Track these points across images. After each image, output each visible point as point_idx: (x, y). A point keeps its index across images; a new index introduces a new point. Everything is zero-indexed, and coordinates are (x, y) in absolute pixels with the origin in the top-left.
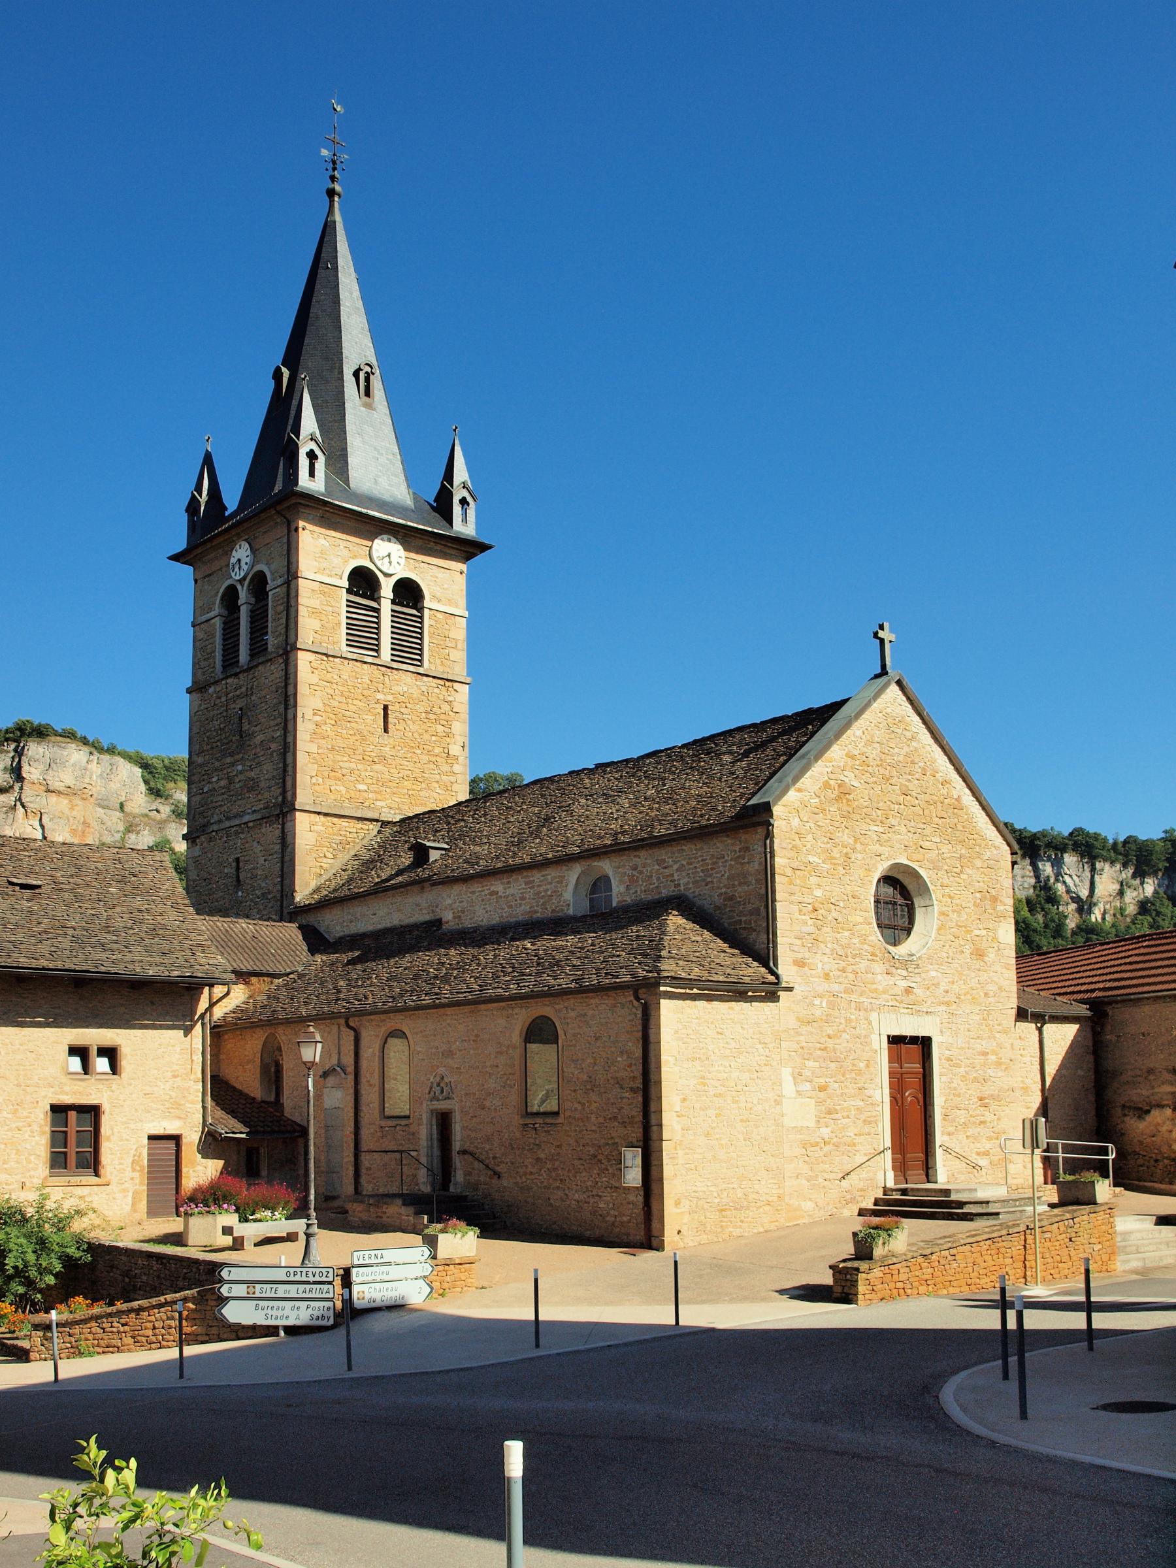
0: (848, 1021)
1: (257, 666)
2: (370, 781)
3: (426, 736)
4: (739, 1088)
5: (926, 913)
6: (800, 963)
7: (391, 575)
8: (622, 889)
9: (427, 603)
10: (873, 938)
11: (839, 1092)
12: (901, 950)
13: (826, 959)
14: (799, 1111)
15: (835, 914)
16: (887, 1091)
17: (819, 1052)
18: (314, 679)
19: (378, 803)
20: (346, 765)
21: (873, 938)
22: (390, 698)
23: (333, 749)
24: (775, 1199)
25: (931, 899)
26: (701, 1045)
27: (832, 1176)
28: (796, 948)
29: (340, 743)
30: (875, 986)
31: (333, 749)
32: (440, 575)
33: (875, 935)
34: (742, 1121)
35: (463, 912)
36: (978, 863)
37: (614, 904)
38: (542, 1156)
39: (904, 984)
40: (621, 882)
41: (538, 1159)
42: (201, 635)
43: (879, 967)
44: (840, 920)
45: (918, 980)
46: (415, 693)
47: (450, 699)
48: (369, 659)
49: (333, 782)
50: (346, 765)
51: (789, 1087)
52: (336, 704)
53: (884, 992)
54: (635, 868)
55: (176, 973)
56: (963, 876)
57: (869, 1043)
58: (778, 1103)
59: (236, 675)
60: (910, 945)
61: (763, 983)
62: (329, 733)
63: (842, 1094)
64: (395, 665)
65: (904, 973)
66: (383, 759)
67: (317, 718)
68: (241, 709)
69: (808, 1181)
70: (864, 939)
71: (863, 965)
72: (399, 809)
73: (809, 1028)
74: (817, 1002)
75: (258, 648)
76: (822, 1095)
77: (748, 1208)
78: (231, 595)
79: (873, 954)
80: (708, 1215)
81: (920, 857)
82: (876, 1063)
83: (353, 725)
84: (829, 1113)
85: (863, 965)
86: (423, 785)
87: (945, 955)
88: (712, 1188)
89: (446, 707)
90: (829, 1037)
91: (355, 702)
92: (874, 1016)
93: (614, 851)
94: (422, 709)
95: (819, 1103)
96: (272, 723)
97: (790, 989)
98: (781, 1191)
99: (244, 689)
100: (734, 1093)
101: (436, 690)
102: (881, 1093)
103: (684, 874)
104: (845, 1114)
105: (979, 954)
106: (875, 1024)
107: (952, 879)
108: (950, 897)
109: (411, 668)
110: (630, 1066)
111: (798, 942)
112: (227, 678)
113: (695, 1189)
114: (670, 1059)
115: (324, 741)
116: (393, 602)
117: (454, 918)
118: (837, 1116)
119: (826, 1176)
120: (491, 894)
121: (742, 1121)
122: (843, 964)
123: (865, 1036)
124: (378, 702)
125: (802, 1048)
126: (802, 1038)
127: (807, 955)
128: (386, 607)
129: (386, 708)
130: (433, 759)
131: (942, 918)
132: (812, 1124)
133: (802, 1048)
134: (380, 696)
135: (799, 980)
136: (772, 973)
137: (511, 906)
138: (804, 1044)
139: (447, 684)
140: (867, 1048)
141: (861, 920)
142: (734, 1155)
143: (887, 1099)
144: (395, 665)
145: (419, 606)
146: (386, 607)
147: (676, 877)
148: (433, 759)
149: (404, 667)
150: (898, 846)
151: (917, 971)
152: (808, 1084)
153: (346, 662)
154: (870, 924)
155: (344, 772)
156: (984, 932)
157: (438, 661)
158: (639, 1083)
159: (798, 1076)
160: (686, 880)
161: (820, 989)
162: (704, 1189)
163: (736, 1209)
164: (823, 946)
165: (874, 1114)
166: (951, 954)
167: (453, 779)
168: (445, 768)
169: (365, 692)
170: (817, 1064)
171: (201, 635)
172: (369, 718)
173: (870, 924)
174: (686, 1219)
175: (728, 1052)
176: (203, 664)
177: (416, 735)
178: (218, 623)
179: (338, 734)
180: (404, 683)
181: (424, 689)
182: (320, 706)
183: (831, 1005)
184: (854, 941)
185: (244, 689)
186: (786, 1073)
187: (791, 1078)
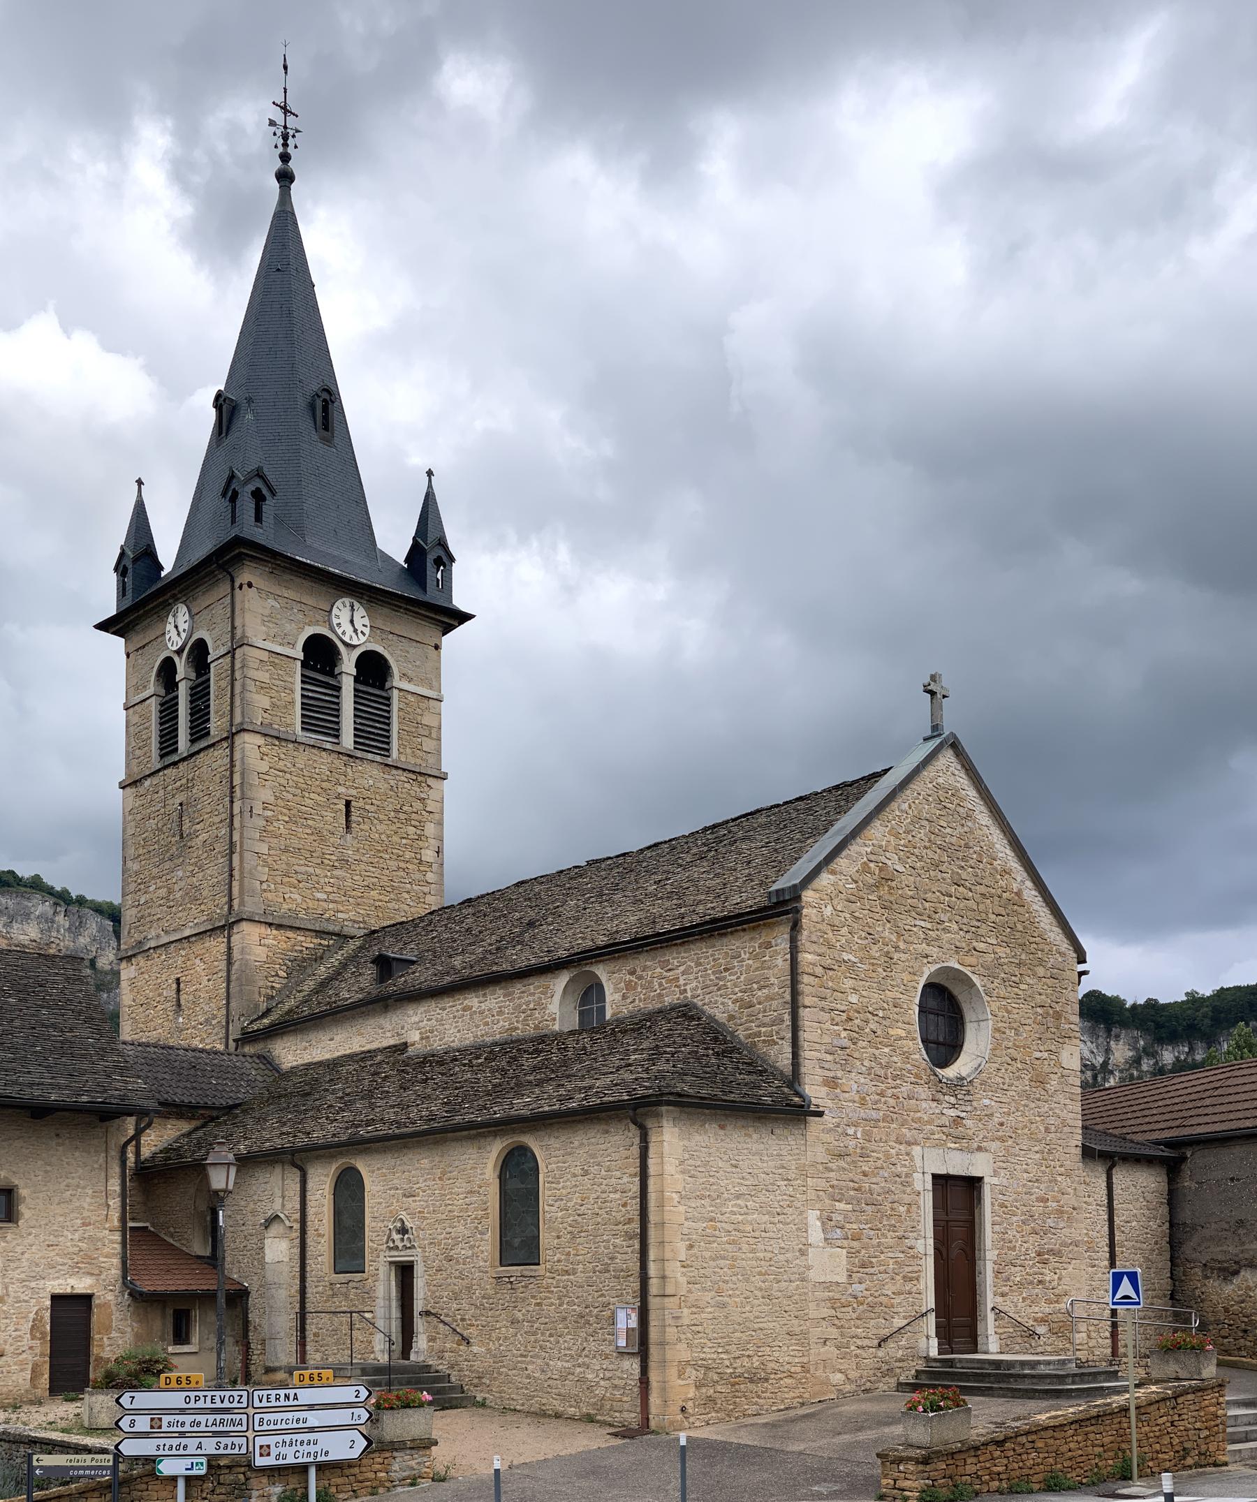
0: (887, 1156)
1: (198, 752)
2: (330, 889)
3: (395, 839)
4: (757, 1234)
5: (978, 1030)
6: (832, 1083)
7: (355, 647)
8: (618, 997)
9: (397, 681)
10: (917, 1056)
11: (875, 1242)
12: (950, 1072)
13: (862, 1080)
14: (828, 1264)
15: (873, 1026)
16: (931, 1242)
17: (852, 1193)
18: (264, 766)
19: (340, 915)
20: (303, 869)
21: (917, 1056)
22: (354, 792)
24: (799, 1369)
25: (984, 1012)
26: (711, 1180)
27: (866, 1342)
28: (826, 1066)
29: (295, 842)
30: (919, 1115)
31: (286, 850)
32: (412, 650)
33: (919, 1054)
34: (760, 1274)
35: (431, 1032)
36: (1041, 971)
37: (608, 1017)
38: (519, 1316)
39: (953, 1113)
40: (617, 990)
41: (514, 1322)
42: (135, 719)
43: (923, 1092)
44: (879, 1033)
45: (969, 1108)
46: (383, 786)
47: (422, 796)
48: (328, 746)
49: (288, 889)
50: (303, 869)
51: (815, 1234)
53: (930, 1122)
54: (632, 973)
55: (85, 1098)
56: (1023, 987)
57: (909, 1184)
58: (803, 1253)
59: (175, 764)
60: (962, 1067)
61: (787, 1105)
62: (282, 830)
63: (879, 1244)
64: (359, 754)
65: (953, 1100)
66: (344, 861)
67: (269, 813)
68: (181, 804)
69: (838, 1348)
70: (906, 1056)
71: (906, 1089)
72: (364, 922)
73: (842, 1163)
74: (851, 1131)
75: (199, 730)
76: (855, 1244)
77: (767, 1380)
78: (167, 669)
79: (917, 1076)
80: (719, 1388)
81: (972, 960)
82: (919, 1207)
83: (310, 822)
84: (863, 1266)
85: (906, 1089)
86: (392, 896)
87: (1000, 1080)
88: (722, 1356)
89: (418, 805)
90: (865, 1174)
91: (312, 795)
92: (916, 1150)
93: (609, 953)
94: (391, 807)
95: (851, 1254)
96: (217, 819)
97: (820, 1114)
98: (805, 1360)
99: (184, 781)
100: (752, 1241)
101: (406, 785)
102: (925, 1244)
103: (691, 977)
104: (882, 1268)
105: (1040, 1081)
106: (918, 1163)
107: (1009, 989)
108: (1008, 1012)
109: (378, 758)
110: (625, 1205)
111: (829, 1058)
112: (165, 768)
113: (703, 1356)
114: (674, 1195)
115: (276, 841)
116: (357, 680)
117: (422, 1039)
118: (872, 1270)
119: (859, 1342)
120: (464, 1010)
121: (760, 1274)
122: (883, 1086)
123: (907, 1175)
125: (832, 1187)
126: (832, 1174)
127: (839, 1074)
128: (348, 685)
129: (348, 804)
130: (402, 865)
131: (997, 1035)
132: (842, 1278)
133: (832, 1187)
134: (341, 789)
135: (829, 1103)
136: (798, 1094)
137: (487, 1024)
138: (835, 1183)
139: (420, 779)
140: (908, 1190)
141: (903, 1034)
142: (751, 1316)
143: (931, 1251)
144: (359, 754)
145: (387, 685)
146: (348, 685)
147: (682, 982)
148: (402, 865)
149: (370, 756)
150: (947, 946)
151: (967, 1098)
152: (838, 1231)
154: (914, 1039)
155: (300, 877)
156: (1046, 1055)
157: (409, 751)
158: (635, 1227)
159: (826, 1220)
160: (694, 984)
161: (854, 1117)
162: (715, 1356)
163: (752, 1381)
164: (858, 1063)
165: (916, 1268)
166: (1007, 1080)
167: (426, 889)
168: (418, 876)
169: (325, 785)
170: (849, 1207)
171: (135, 719)
172: (329, 815)
173: (914, 1039)
174: (692, 1393)
175: (743, 1190)
176: (138, 753)
177: (383, 837)
178: (153, 704)
179: (293, 833)
180: (369, 775)
181: (392, 783)
182: (272, 799)
183: (868, 1137)
184: (895, 1059)
185: (184, 781)
186: (813, 1218)
187: (819, 1224)
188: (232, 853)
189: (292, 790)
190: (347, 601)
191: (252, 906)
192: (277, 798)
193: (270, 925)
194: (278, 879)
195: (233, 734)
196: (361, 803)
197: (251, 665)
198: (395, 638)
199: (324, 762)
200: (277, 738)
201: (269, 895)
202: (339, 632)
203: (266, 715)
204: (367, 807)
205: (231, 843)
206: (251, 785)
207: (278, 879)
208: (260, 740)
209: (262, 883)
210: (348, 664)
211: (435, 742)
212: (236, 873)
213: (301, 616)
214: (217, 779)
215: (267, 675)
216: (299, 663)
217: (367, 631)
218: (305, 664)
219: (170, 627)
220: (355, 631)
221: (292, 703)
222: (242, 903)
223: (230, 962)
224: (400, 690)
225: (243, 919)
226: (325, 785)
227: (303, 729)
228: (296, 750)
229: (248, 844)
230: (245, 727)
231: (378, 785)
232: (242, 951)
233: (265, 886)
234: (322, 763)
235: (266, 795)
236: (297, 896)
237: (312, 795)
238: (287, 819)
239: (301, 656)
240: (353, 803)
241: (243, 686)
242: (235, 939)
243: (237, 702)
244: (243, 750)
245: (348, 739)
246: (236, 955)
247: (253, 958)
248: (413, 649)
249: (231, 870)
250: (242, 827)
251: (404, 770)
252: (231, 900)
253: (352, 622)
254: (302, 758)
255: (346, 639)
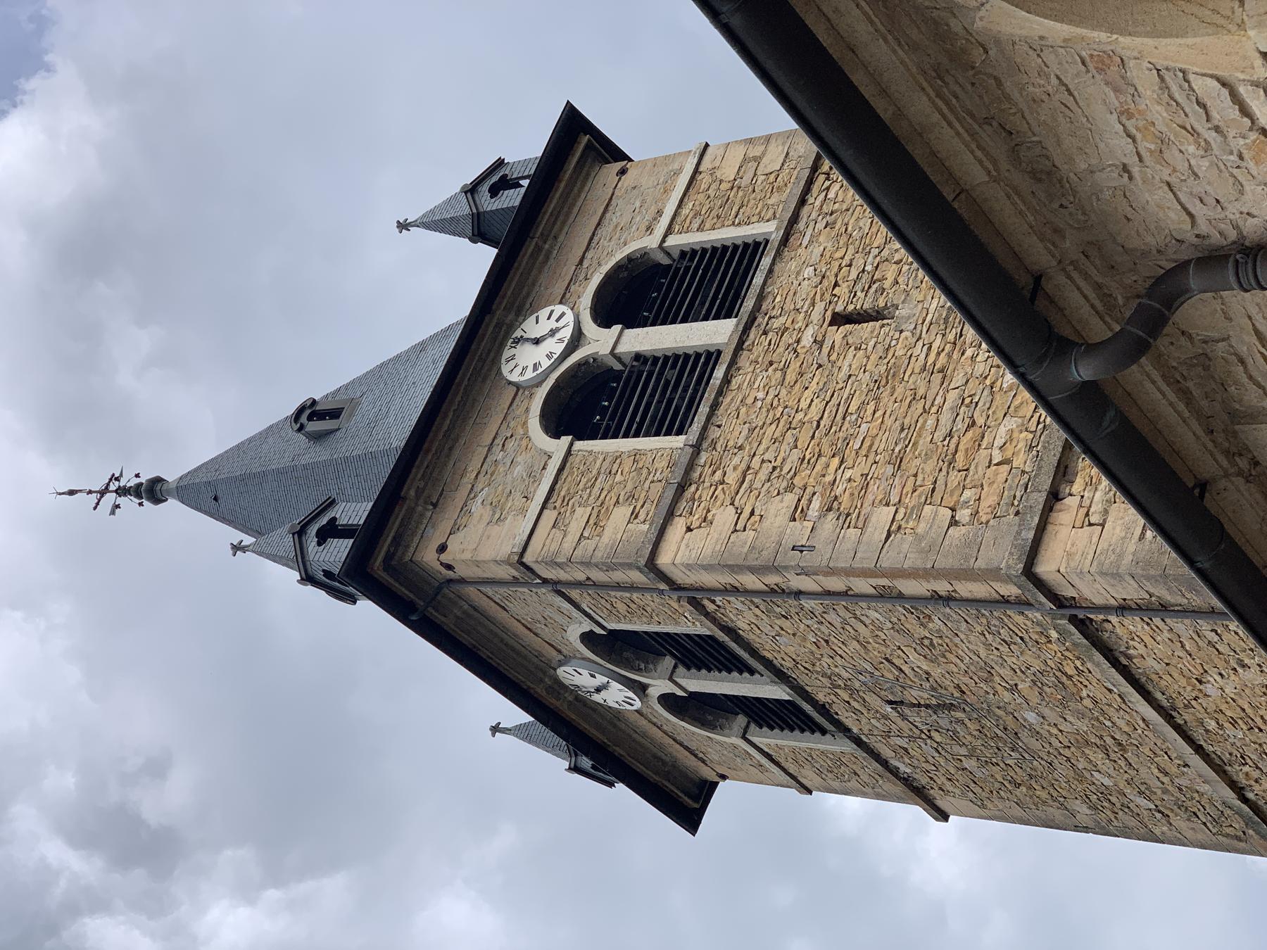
18: (724, 517)
20: (946, 417)
22: (820, 306)
23: (898, 463)
31: (898, 463)
50: (946, 417)
52: (796, 454)
67: (816, 504)
83: (852, 409)
91: (804, 405)
115: (873, 488)
124: (819, 343)
144: (749, 303)
153: (714, 433)
155: (960, 426)
181: (820, 225)
182: (790, 499)
188: (900, 596)
189: (785, 447)
190: (507, 353)
191: (1001, 552)
192: (790, 488)
193: (1054, 497)
194: (955, 478)
195: (675, 586)
196: (843, 290)
197: (554, 547)
198: (589, 255)
199: (752, 384)
200: (681, 488)
201: (984, 504)
202: (546, 363)
203: (642, 517)
204: (853, 275)
205: (883, 595)
206: (752, 548)
207: (955, 478)
208: (679, 524)
209: (954, 522)
210: (602, 341)
211: (772, 147)
212: (942, 587)
213: (510, 445)
214: (786, 624)
215: (579, 511)
216: (579, 445)
217: (559, 309)
218: (580, 437)
219: (597, 698)
220: (553, 332)
221: (636, 455)
222: (993, 574)
223: (1164, 609)
224: (669, 231)
225: (1029, 572)
226: (791, 377)
227: (679, 433)
228: (713, 444)
229: (865, 560)
230: (642, 562)
231: (818, 251)
232: (1115, 576)
233: (963, 515)
234: (751, 384)
235: (777, 510)
236: (1002, 430)
237: (804, 405)
238: (836, 461)
239: (566, 440)
240: (839, 308)
241: (587, 564)
242: (1094, 591)
243: (618, 576)
244: (689, 567)
245: (713, 333)
246: (1130, 592)
247: (1132, 546)
248: (613, 218)
249: (936, 598)
250: (831, 572)
251: (802, 202)
252: (1005, 601)
253: (537, 342)
254: (730, 429)
255: (559, 349)
